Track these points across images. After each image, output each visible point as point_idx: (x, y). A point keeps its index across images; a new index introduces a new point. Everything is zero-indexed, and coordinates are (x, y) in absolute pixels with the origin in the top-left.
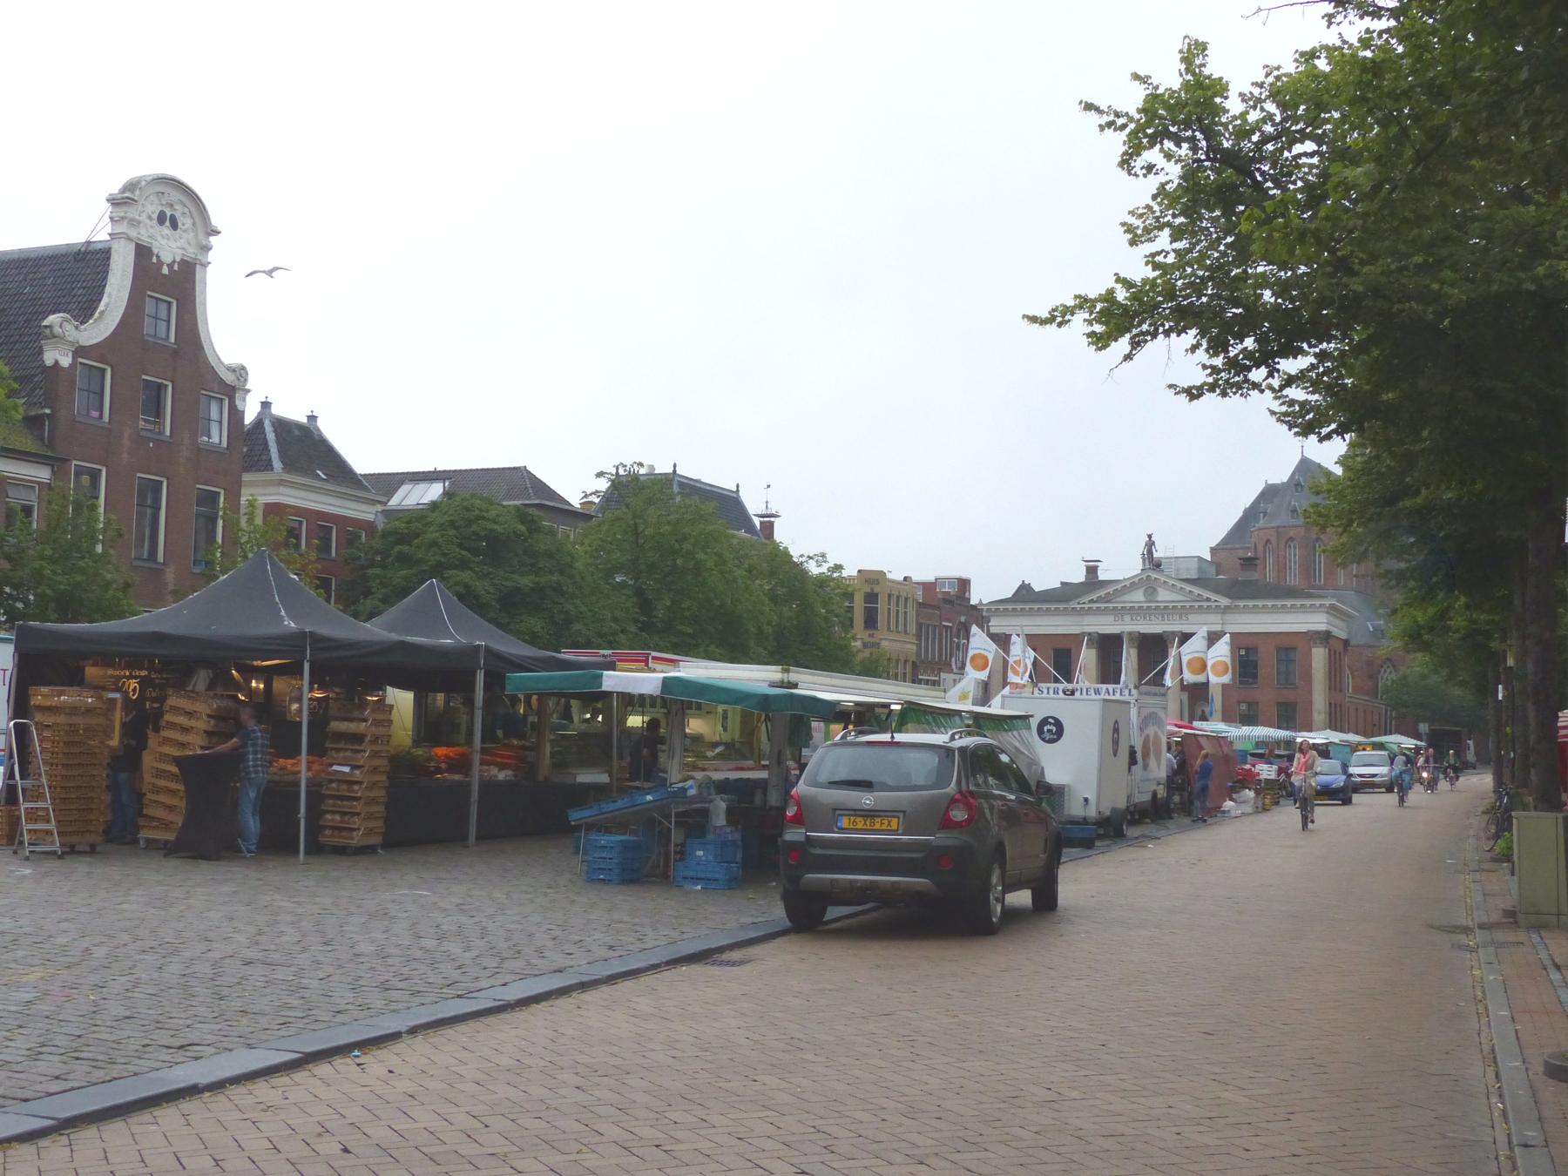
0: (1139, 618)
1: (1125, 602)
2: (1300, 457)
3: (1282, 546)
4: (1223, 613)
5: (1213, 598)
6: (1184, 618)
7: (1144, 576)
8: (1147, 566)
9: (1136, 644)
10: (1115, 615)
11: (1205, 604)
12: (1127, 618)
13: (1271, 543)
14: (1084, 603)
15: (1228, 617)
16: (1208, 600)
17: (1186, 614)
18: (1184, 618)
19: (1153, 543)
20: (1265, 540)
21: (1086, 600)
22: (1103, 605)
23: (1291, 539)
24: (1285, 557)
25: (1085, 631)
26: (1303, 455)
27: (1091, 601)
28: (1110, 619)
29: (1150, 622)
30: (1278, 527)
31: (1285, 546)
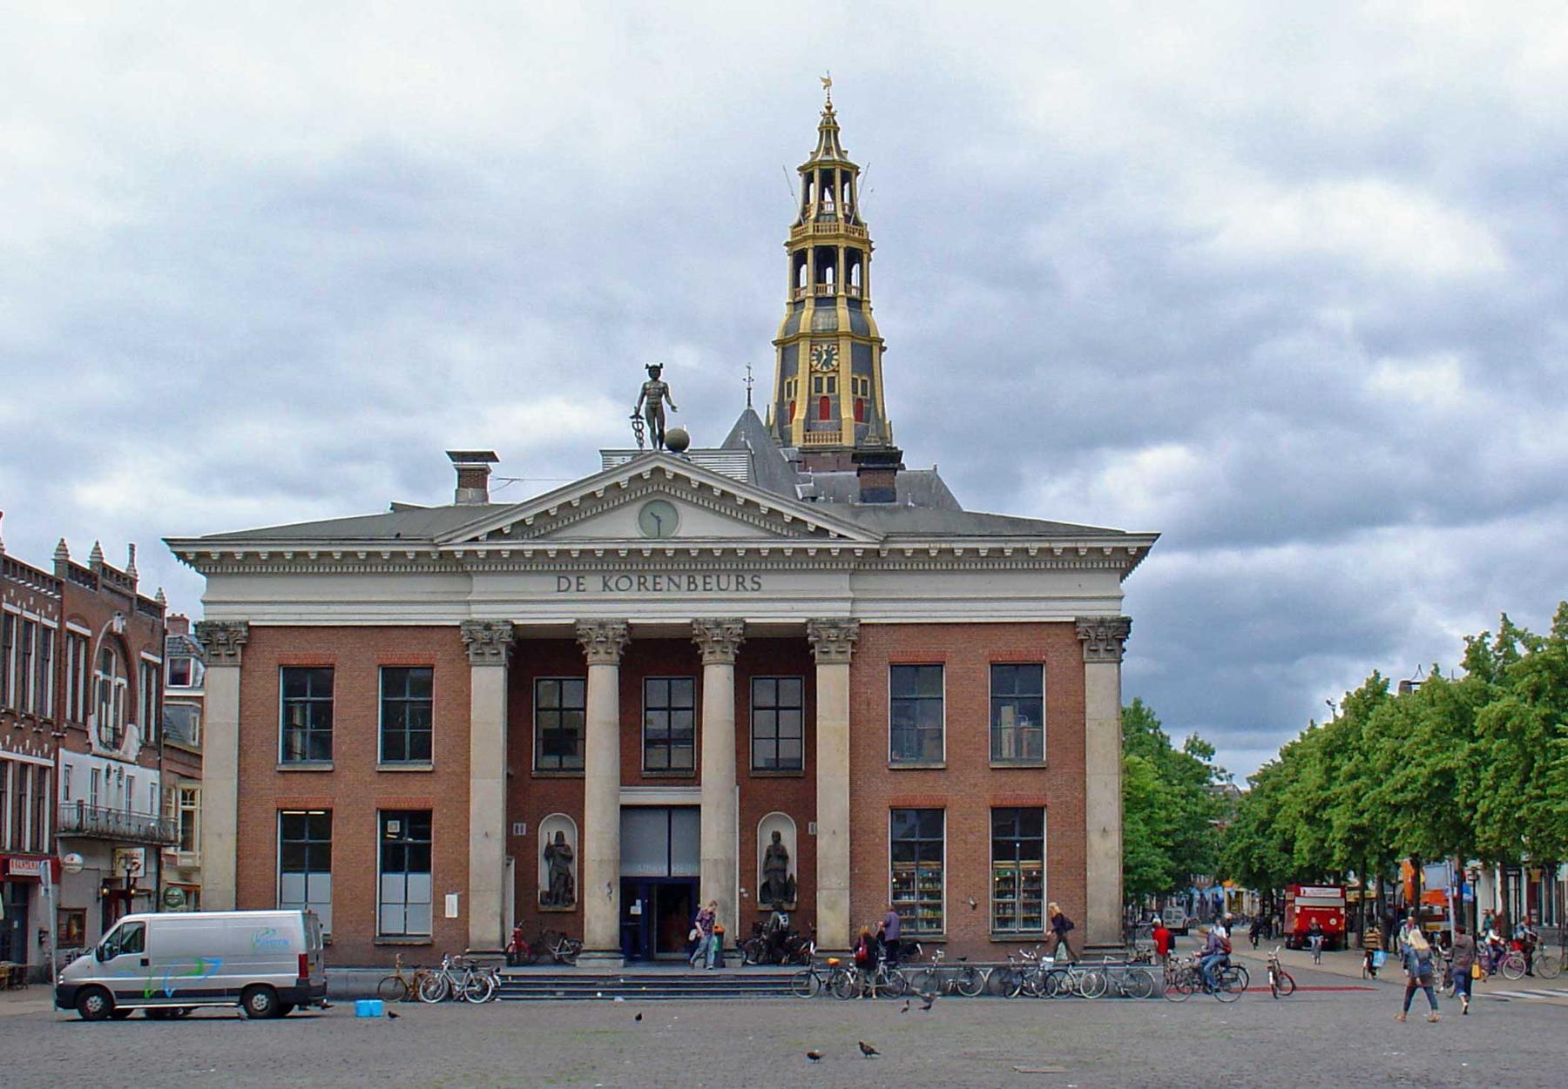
0: (624, 583)
1: (591, 540)
4: (854, 572)
5: (834, 530)
6: (748, 584)
7: (645, 470)
8: (648, 445)
9: (616, 658)
10: (561, 575)
11: (812, 545)
12: (593, 583)
14: (476, 539)
15: (873, 584)
16: (821, 532)
17: (756, 573)
18: (748, 584)
19: (664, 390)
21: (481, 533)
22: (529, 547)
25: (475, 616)
26: (749, 404)
27: (496, 534)
28: (544, 586)
29: (658, 595)
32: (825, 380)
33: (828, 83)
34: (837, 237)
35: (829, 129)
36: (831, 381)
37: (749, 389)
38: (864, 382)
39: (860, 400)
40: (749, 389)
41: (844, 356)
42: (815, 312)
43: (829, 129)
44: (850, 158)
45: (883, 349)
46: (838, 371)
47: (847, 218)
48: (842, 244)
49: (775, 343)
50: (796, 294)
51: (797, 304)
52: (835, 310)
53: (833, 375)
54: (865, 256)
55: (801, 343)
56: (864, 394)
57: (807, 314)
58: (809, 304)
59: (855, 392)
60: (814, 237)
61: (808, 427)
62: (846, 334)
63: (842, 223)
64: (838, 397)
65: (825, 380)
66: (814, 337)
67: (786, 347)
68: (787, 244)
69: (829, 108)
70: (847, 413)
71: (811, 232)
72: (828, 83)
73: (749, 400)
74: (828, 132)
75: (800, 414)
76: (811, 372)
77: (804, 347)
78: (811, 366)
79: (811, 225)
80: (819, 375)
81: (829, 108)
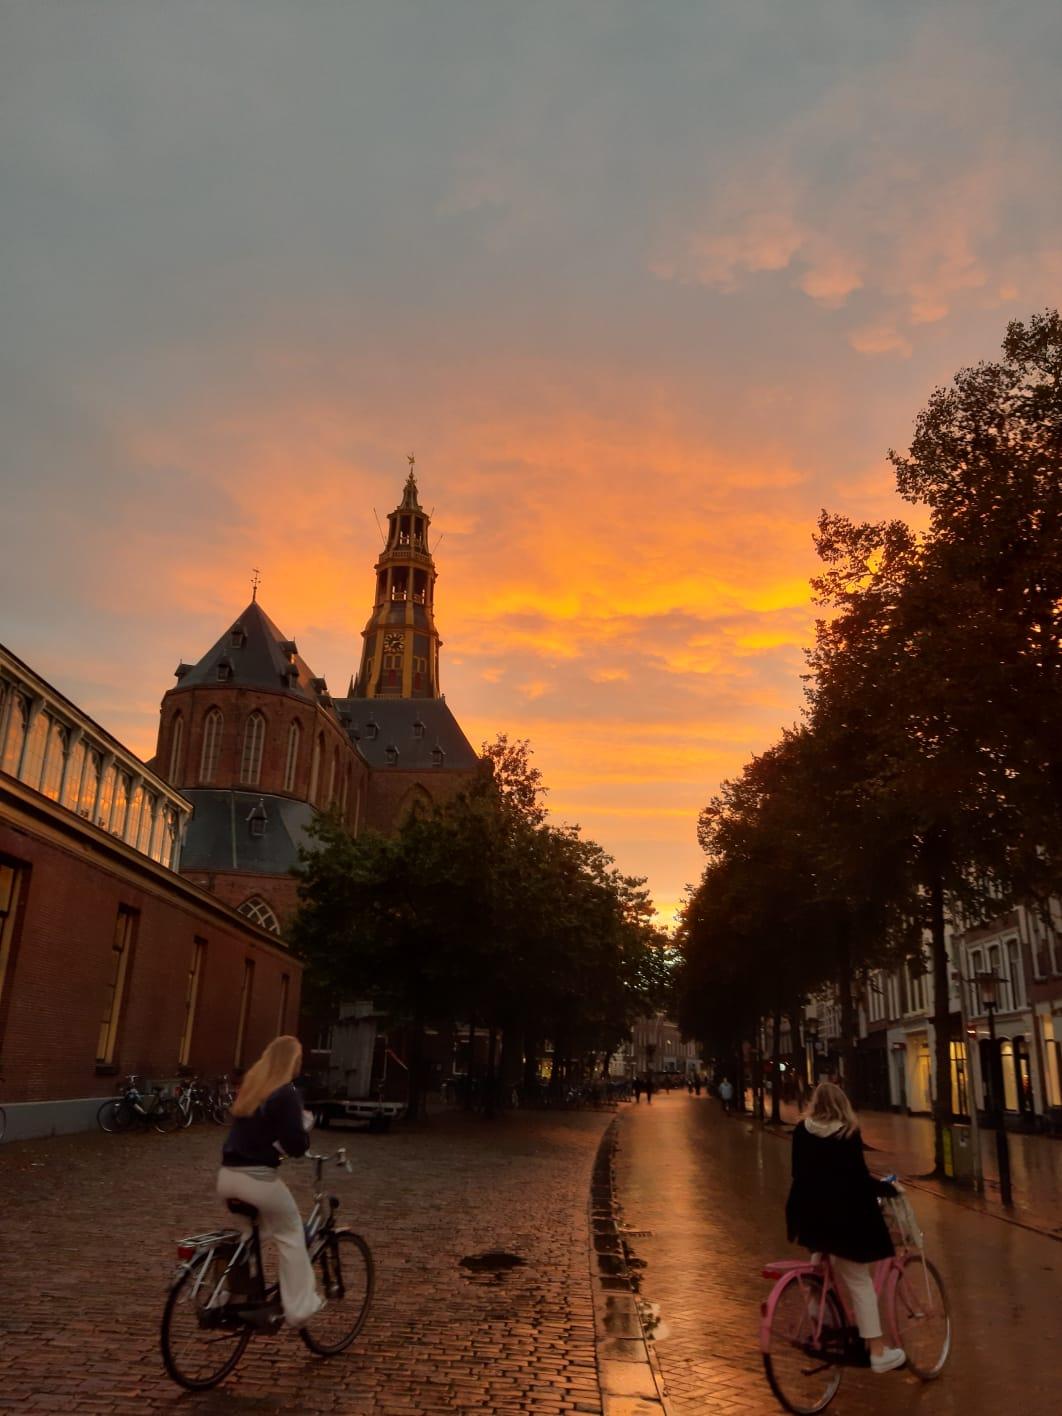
2: (250, 602)
3: (198, 717)
13: (183, 717)
20: (174, 710)
23: (214, 707)
24: (201, 736)
30: (195, 689)
31: (204, 718)
32: (394, 659)
33: (412, 461)
34: (409, 559)
35: (411, 491)
36: (398, 659)
37: (255, 588)
38: (422, 662)
39: (418, 674)
40: (255, 588)
41: (408, 642)
42: (390, 612)
43: (411, 491)
44: (423, 511)
45: (439, 644)
46: (402, 653)
47: (417, 549)
48: (412, 565)
49: (363, 634)
50: (378, 599)
51: (378, 607)
52: (405, 611)
53: (398, 655)
54: (430, 577)
55: (379, 632)
56: (422, 669)
57: (384, 613)
58: (387, 606)
59: (415, 667)
60: (393, 560)
61: (379, 689)
62: (410, 626)
63: (413, 551)
64: (401, 671)
65: (394, 659)
66: (387, 627)
67: (370, 635)
68: (376, 567)
69: (411, 477)
70: (407, 680)
71: (390, 556)
72: (412, 461)
73: (254, 597)
74: (409, 492)
75: (374, 681)
76: (384, 653)
77: (380, 635)
78: (384, 648)
79: (391, 552)
80: (390, 655)
81: (411, 477)
